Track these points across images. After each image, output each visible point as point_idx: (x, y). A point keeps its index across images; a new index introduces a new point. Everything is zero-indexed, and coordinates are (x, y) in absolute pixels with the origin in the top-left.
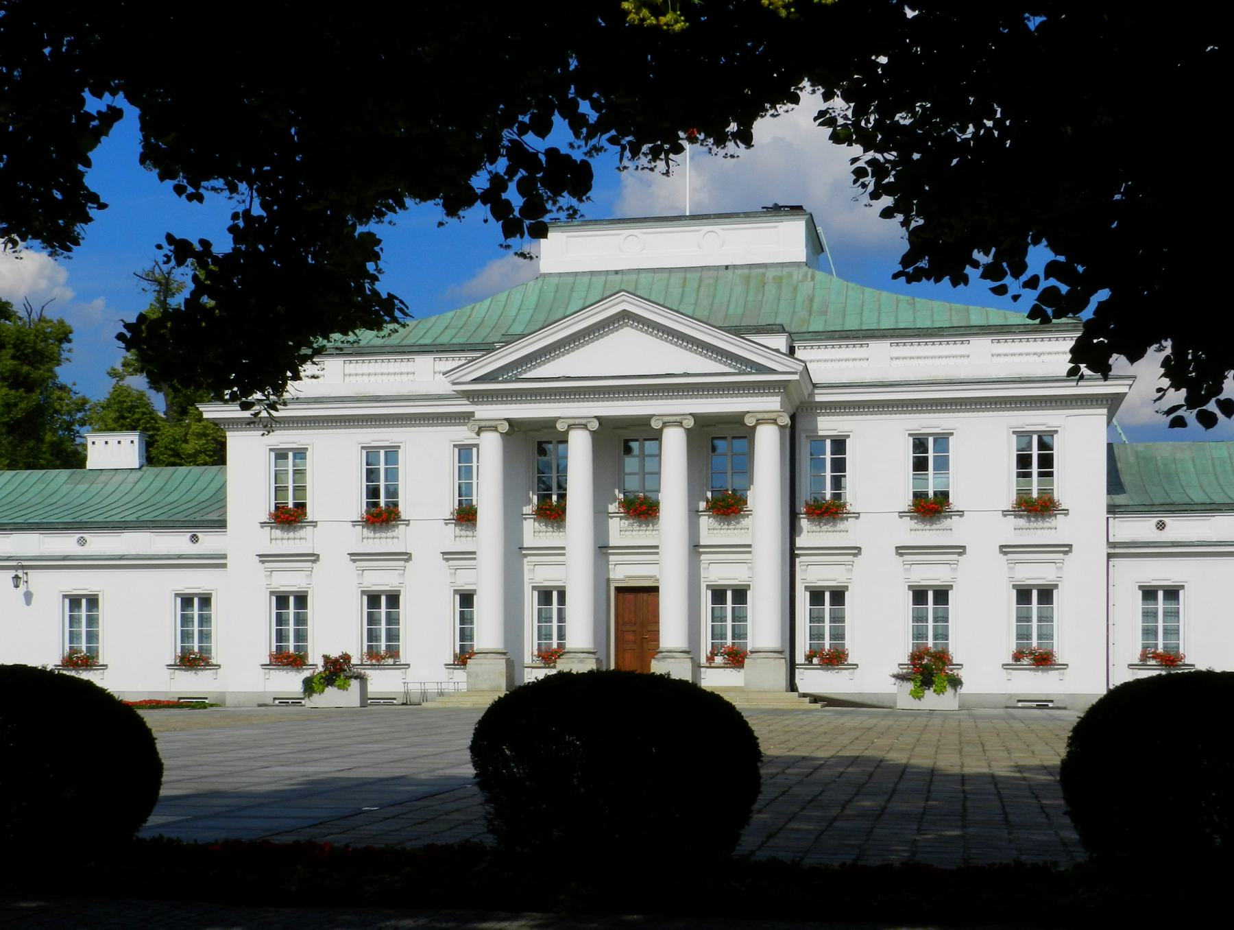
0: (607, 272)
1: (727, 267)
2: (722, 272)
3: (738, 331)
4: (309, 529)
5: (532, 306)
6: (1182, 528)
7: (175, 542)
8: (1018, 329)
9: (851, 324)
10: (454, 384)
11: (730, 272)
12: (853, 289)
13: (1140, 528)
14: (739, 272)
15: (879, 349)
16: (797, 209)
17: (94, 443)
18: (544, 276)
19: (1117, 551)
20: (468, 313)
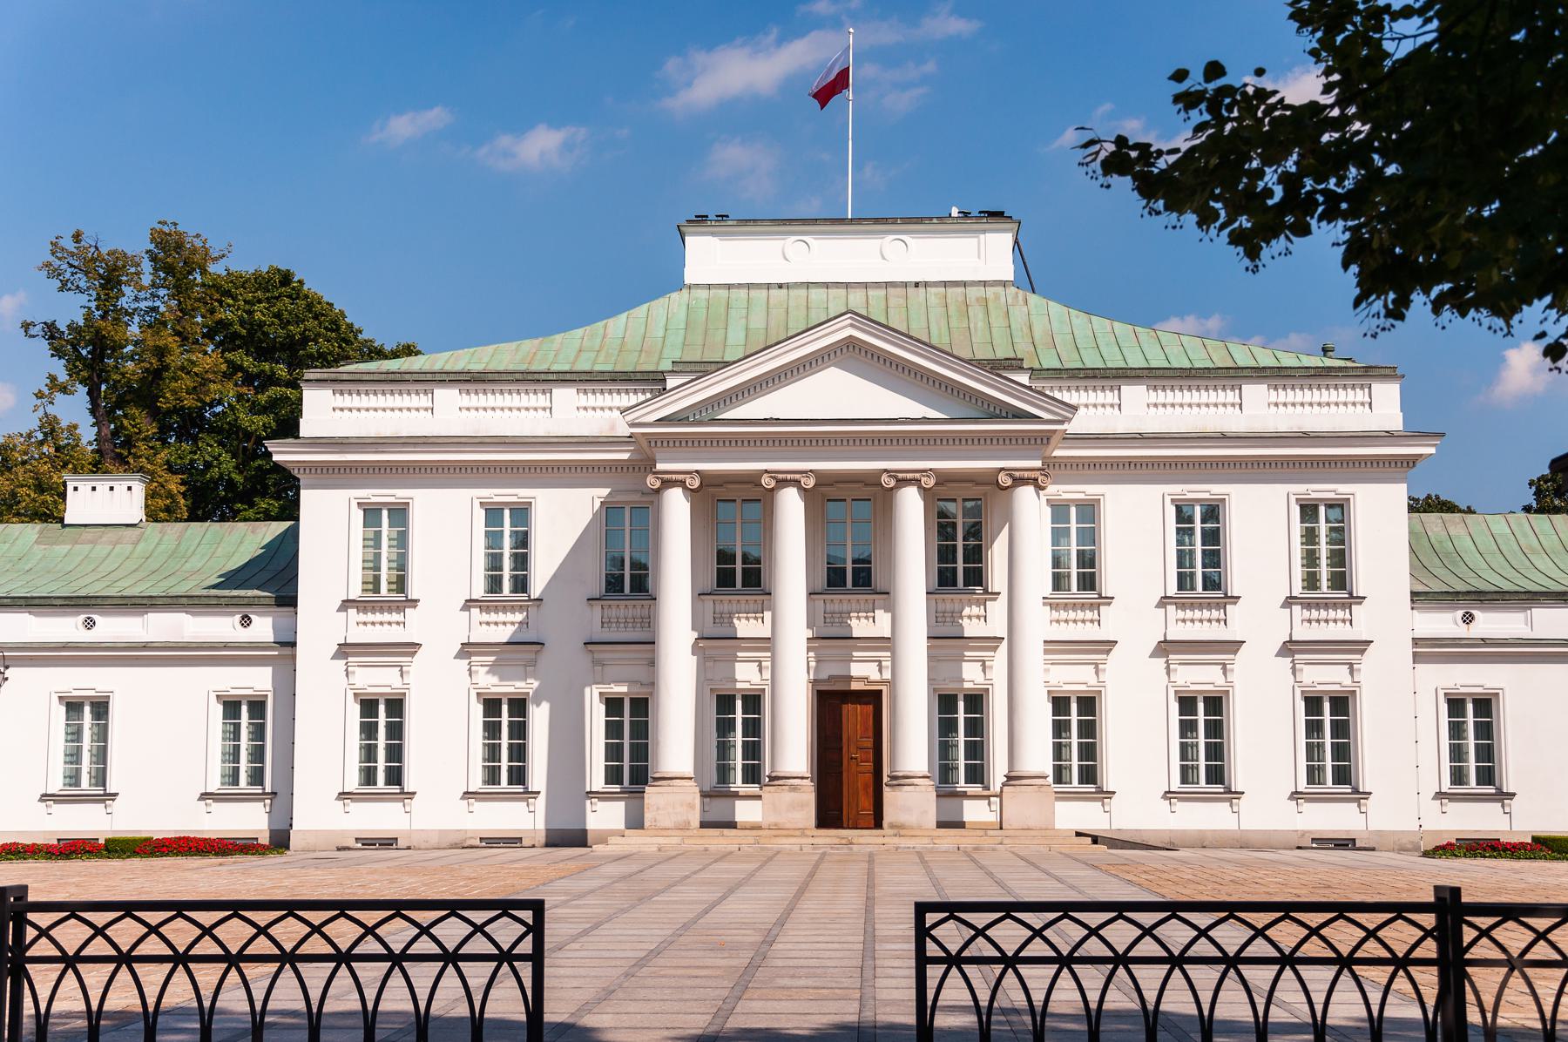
0: (769, 286)
1: (917, 285)
2: (911, 290)
5: (683, 326)
6: (1492, 624)
7: (221, 627)
8: (1341, 372)
9: (1092, 361)
10: (632, 425)
11: (921, 290)
12: (1077, 317)
14: (931, 290)
15: (1135, 394)
16: (996, 215)
17: (76, 489)
18: (690, 287)
19: (1428, 650)
20: (601, 331)
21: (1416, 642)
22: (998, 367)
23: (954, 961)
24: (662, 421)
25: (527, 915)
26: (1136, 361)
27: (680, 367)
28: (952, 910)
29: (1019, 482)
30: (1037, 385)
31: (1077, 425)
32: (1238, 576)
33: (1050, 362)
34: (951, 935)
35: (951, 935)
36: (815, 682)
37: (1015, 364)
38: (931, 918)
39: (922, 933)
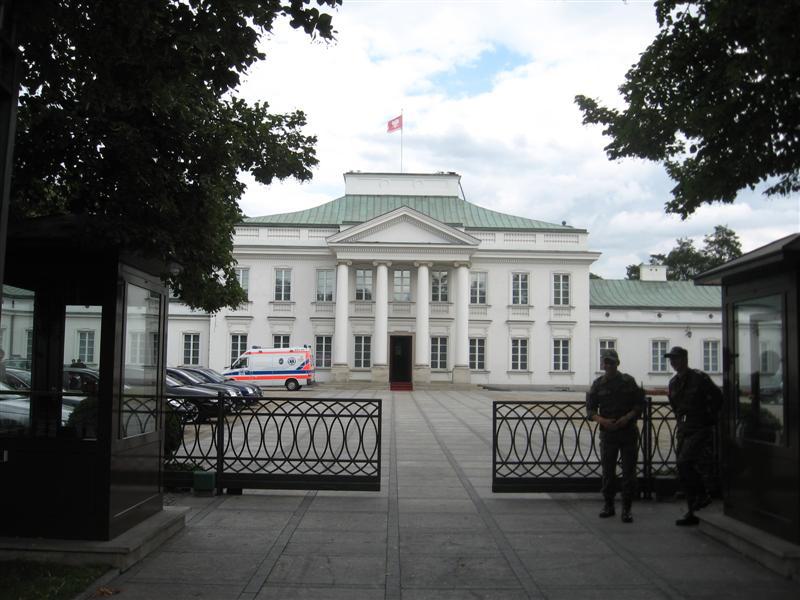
3: (454, 225)
4: (249, 305)
6: (616, 316)
13: (600, 316)
15: (500, 236)
21: (591, 322)
22: (454, 225)
23: (504, 418)
24: (338, 242)
25: (377, 404)
26: (500, 225)
27: (345, 223)
28: (504, 403)
29: (461, 266)
30: (468, 232)
31: (481, 246)
32: (533, 297)
33: (471, 225)
34: (504, 411)
35: (504, 411)
36: (388, 333)
37: (461, 225)
38: (498, 406)
39: (495, 410)
